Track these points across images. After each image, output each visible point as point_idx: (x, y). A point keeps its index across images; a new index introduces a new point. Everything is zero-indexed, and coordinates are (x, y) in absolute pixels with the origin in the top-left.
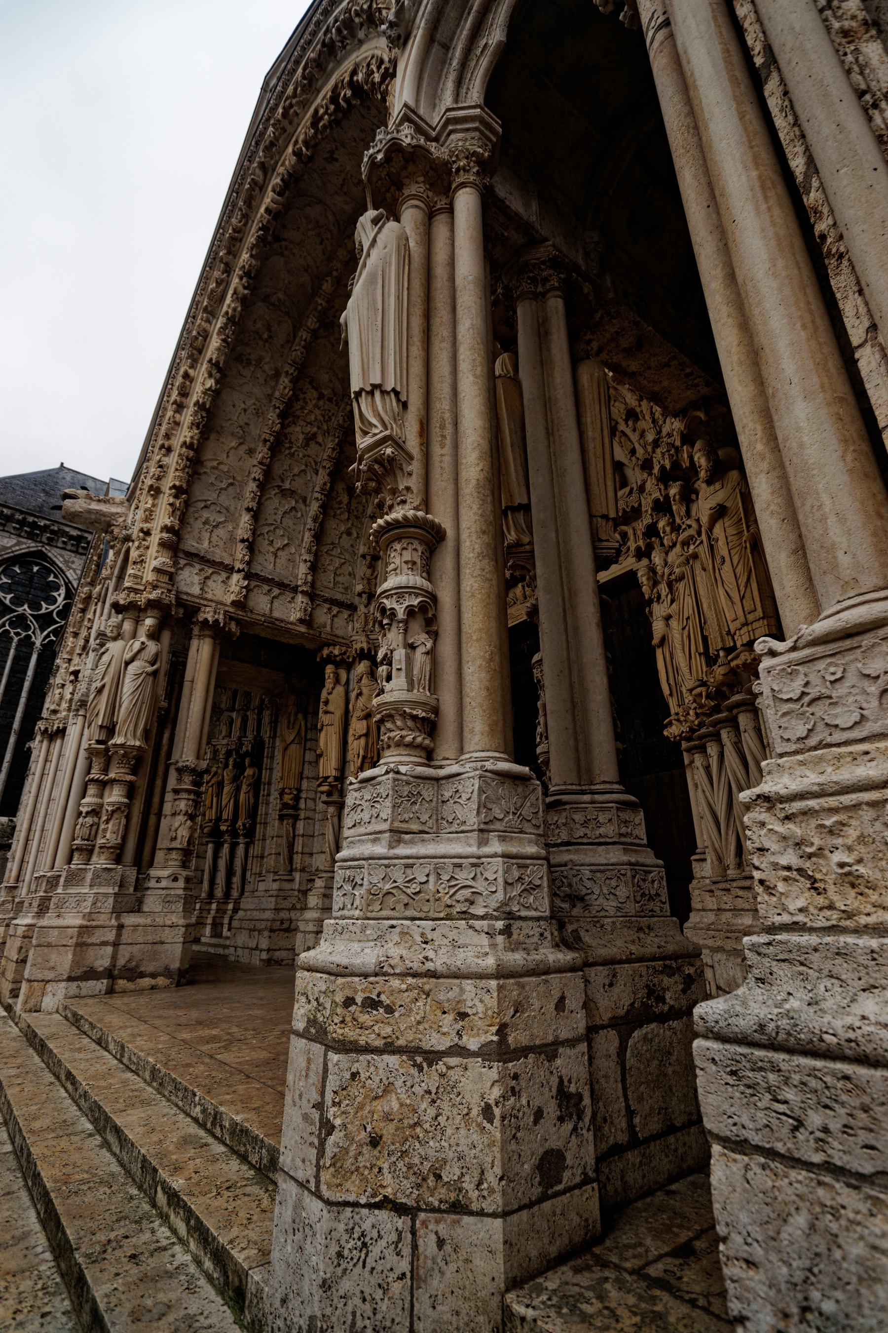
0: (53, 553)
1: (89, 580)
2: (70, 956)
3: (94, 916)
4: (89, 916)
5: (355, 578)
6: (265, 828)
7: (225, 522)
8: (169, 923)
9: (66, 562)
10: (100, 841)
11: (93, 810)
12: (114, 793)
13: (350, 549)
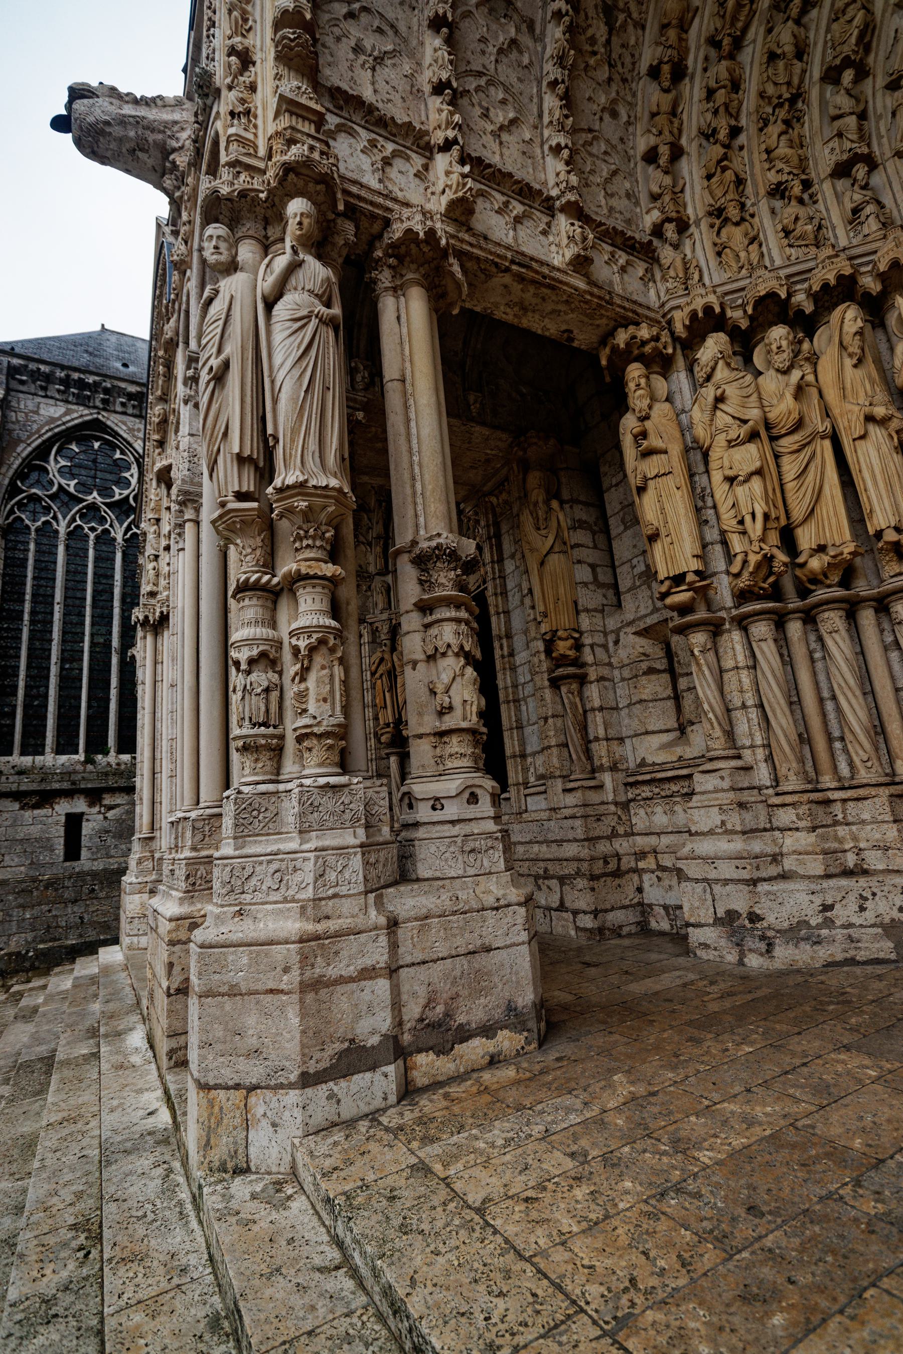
0: (112, 420)
1: (159, 393)
2: (294, 1020)
3: (328, 907)
4: (314, 908)
5: (637, 203)
6: (518, 710)
7: (393, 54)
8: (490, 901)
9: (131, 430)
10: (292, 724)
11: (263, 655)
12: (302, 607)
13: (620, 147)
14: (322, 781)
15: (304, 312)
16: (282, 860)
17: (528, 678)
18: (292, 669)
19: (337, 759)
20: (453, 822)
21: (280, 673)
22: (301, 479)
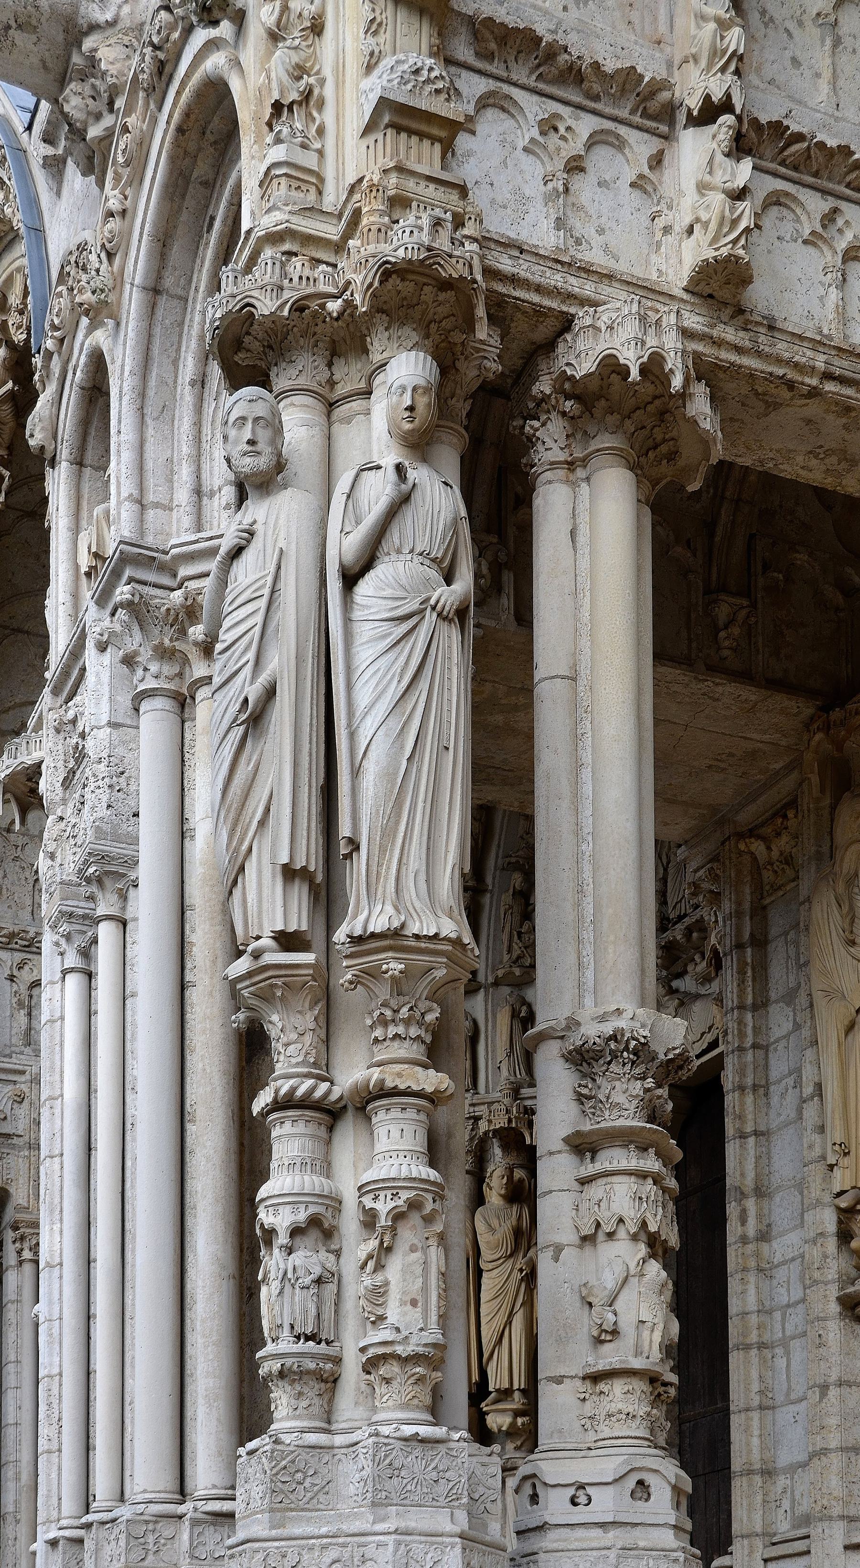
11: (314, 1221)
14: (408, 1430)
15: (414, 605)
16: (344, 1545)
17: (797, 1293)
18: (357, 1246)
19: (428, 1400)
20: (602, 1525)
21: (338, 1253)
22: (396, 924)
